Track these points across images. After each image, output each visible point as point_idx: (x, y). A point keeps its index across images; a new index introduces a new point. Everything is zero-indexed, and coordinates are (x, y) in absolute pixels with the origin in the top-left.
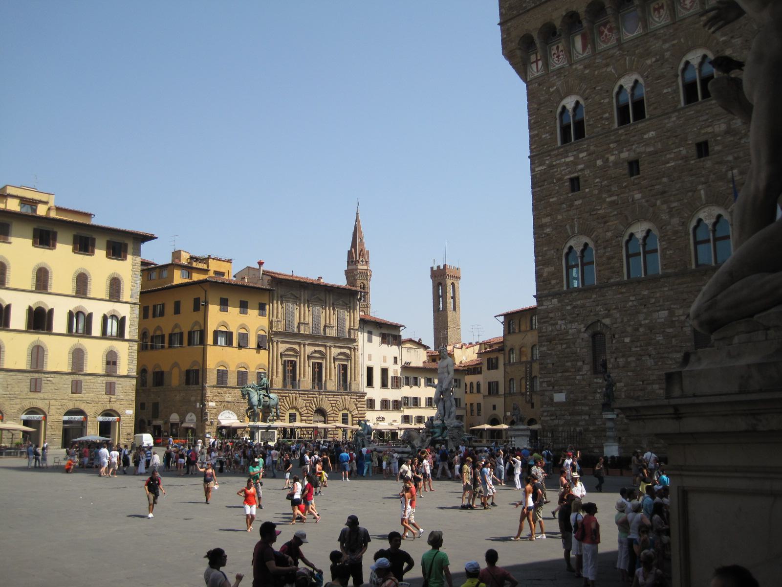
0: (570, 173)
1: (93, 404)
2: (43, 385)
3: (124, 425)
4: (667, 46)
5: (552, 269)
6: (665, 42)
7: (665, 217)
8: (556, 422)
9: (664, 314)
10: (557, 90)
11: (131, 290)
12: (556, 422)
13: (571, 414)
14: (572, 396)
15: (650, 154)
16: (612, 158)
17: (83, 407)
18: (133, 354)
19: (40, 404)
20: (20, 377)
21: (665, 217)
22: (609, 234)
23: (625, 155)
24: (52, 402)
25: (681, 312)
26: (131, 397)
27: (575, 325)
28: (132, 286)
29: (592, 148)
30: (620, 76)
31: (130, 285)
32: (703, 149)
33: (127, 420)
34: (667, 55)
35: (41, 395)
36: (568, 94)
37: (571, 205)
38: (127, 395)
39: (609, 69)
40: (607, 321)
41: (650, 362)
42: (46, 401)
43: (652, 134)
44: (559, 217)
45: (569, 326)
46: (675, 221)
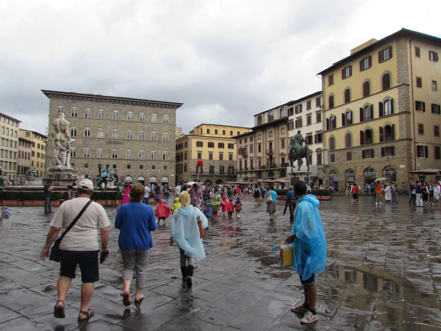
1: (378, 164)
2: (352, 155)
3: (400, 176)
11: (398, 77)
17: (372, 166)
18: (402, 123)
19: (352, 167)
20: (342, 153)
24: (357, 165)
26: (403, 155)
28: (398, 74)
31: (396, 73)
33: (402, 172)
35: (352, 161)
38: (400, 154)
42: (354, 165)
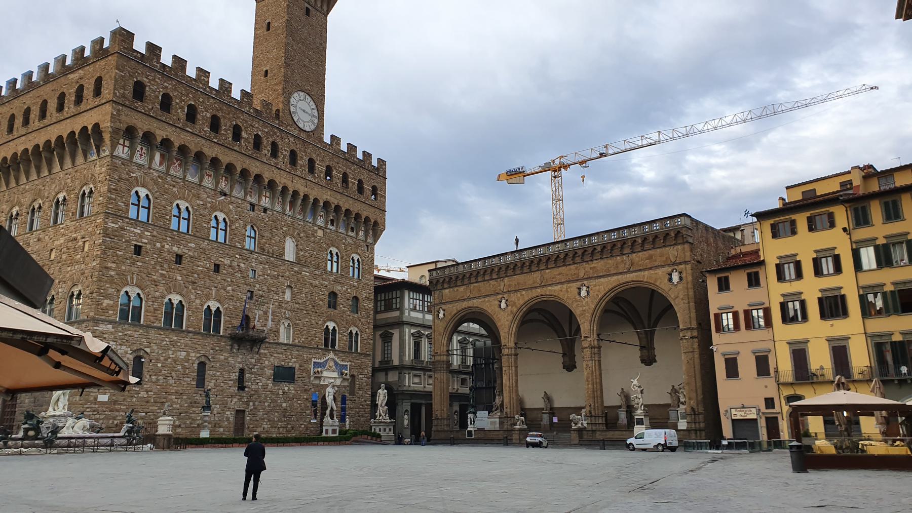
0: (136, 241)
4: (209, 200)
5: (111, 302)
6: (208, 197)
7: (193, 297)
8: (98, 416)
9: (184, 354)
10: (136, 178)
12: (98, 416)
13: (111, 411)
14: (114, 398)
15: (190, 256)
16: (167, 246)
21: (193, 297)
22: (157, 294)
23: (175, 249)
25: (193, 355)
27: (124, 348)
29: (155, 233)
30: (180, 198)
32: (217, 268)
34: (209, 205)
36: (143, 186)
37: (134, 264)
39: (175, 189)
40: (148, 350)
41: (172, 382)
43: (192, 245)
44: (123, 268)
45: (119, 347)
46: (198, 301)
